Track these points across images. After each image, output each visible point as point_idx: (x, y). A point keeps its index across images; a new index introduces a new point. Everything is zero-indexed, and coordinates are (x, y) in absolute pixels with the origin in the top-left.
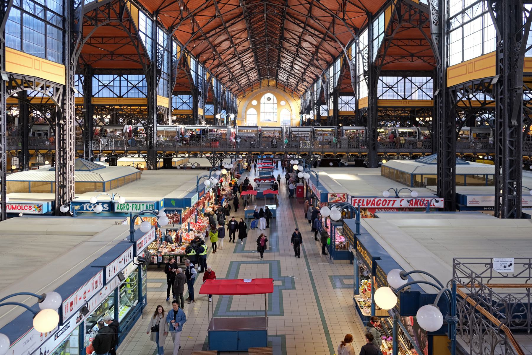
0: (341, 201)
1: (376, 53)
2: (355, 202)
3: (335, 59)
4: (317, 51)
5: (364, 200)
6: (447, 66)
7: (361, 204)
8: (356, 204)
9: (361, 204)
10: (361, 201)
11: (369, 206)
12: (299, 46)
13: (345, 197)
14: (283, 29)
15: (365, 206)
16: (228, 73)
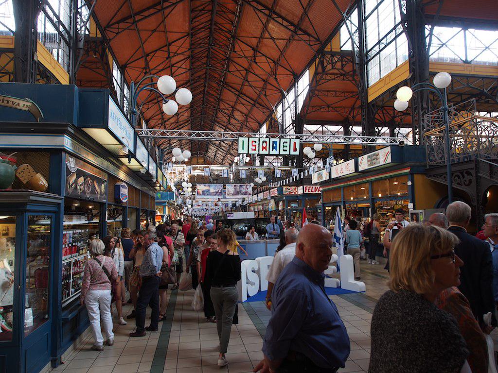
0: (293, 193)
1: (302, 104)
2: (306, 189)
3: (260, 126)
4: (246, 120)
5: (312, 187)
6: (368, 87)
7: (310, 190)
8: (307, 190)
9: (310, 190)
10: (311, 188)
11: (317, 192)
12: (231, 116)
13: (296, 190)
14: (219, 100)
15: (314, 192)
16: (168, 145)
